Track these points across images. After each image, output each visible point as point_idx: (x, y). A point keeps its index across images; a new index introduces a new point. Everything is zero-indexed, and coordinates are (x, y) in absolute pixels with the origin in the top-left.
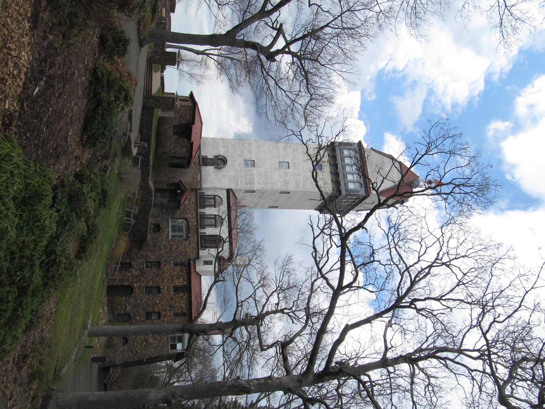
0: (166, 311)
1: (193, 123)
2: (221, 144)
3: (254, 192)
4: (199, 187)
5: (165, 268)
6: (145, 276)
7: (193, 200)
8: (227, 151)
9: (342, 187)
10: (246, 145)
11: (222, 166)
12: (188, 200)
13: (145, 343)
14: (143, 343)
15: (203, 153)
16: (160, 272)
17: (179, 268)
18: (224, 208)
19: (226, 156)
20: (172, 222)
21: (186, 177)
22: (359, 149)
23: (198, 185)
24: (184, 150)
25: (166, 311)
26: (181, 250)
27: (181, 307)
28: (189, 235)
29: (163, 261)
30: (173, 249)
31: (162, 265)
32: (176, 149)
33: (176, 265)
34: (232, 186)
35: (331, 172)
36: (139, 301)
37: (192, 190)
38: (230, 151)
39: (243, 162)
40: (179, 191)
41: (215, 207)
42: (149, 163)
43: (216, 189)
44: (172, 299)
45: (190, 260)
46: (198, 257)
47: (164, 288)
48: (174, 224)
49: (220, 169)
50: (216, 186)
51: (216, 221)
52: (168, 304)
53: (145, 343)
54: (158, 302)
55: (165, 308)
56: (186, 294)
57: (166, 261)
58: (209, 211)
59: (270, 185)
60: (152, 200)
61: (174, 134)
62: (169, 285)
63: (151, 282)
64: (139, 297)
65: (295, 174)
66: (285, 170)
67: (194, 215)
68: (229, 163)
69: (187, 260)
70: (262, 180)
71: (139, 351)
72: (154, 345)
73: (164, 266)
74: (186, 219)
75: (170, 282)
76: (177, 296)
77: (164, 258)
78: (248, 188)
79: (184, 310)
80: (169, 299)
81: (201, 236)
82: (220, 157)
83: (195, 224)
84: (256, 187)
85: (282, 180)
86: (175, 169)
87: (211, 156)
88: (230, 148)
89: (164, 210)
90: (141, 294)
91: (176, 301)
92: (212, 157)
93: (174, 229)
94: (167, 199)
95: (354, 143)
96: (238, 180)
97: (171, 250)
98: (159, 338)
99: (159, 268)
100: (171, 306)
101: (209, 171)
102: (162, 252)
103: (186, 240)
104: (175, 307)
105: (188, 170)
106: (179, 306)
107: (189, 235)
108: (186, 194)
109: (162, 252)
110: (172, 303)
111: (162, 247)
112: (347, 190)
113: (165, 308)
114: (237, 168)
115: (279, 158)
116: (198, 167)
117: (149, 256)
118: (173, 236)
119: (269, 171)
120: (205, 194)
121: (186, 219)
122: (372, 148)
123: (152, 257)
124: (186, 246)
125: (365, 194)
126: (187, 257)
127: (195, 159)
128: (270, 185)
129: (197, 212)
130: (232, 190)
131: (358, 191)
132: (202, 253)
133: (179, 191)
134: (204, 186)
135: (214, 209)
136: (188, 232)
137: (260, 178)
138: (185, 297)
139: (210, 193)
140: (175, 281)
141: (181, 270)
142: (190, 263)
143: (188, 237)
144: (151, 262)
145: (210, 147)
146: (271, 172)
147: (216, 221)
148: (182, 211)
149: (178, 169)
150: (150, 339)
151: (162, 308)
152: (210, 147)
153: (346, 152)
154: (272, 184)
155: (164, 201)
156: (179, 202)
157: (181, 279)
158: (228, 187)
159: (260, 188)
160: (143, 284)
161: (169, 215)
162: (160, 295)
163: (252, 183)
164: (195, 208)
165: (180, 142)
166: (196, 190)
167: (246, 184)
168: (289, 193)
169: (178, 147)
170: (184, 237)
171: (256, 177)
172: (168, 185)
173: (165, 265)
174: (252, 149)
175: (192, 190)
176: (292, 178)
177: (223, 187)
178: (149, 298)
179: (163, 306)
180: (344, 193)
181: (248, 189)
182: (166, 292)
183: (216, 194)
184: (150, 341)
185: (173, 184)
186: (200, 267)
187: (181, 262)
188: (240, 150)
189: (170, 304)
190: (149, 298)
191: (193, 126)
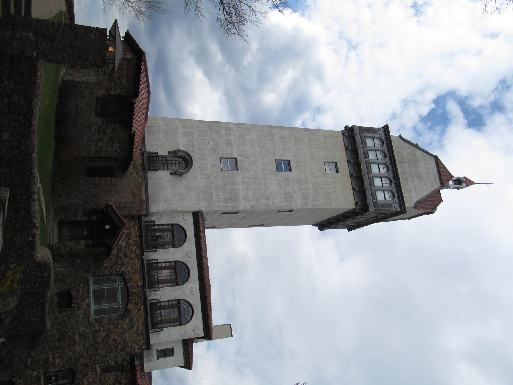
1: (136, 94)
2: (180, 130)
4: (144, 212)
7: (134, 237)
9: (370, 200)
10: (222, 132)
12: (126, 240)
15: (150, 148)
17: (113, 377)
18: (190, 245)
19: (189, 150)
20: (95, 283)
21: (117, 195)
22: (386, 138)
23: (142, 208)
24: (117, 146)
26: (114, 340)
28: (130, 306)
30: (99, 340)
31: (79, 376)
32: (100, 144)
33: (106, 370)
35: (351, 175)
37: (131, 218)
39: (218, 162)
40: (107, 227)
41: (174, 247)
43: (175, 212)
45: (132, 360)
48: (100, 287)
49: (181, 175)
50: (175, 206)
51: (179, 273)
57: (85, 365)
58: (164, 255)
59: (263, 201)
60: (49, 277)
61: (98, 114)
66: (284, 174)
67: (138, 266)
68: (196, 164)
69: (128, 358)
70: (251, 192)
77: (82, 361)
82: (180, 154)
83: (140, 283)
86: (97, 179)
87: (163, 152)
89: (79, 261)
92: (166, 154)
93: (99, 297)
94: (83, 242)
95: (379, 129)
101: (161, 180)
102: (78, 348)
103: (123, 317)
107: (130, 306)
109: (78, 348)
111: (77, 338)
112: (376, 204)
116: (141, 173)
117: (51, 360)
118: (97, 312)
120: (156, 223)
121: (122, 275)
122: (400, 136)
123: (57, 361)
124: (124, 331)
125: (399, 209)
126: (127, 353)
128: (263, 201)
129: (142, 260)
131: (389, 205)
132: (154, 339)
133: (107, 227)
134: (154, 208)
135: (172, 250)
136: (128, 302)
139: (165, 220)
142: (133, 367)
143: (126, 311)
146: (265, 178)
147: (179, 273)
148: (114, 260)
149: (103, 179)
153: (369, 143)
158: (195, 209)
159: (248, 208)
163: (235, 198)
164: (138, 252)
165: (108, 131)
166: (140, 217)
170: (121, 312)
172: (85, 213)
173: (85, 375)
174: (232, 138)
175: (131, 218)
177: (187, 209)
180: (371, 208)
181: (230, 209)
183: (174, 223)
186: (152, 364)
187: (116, 362)
188: (213, 139)
191: (136, 101)
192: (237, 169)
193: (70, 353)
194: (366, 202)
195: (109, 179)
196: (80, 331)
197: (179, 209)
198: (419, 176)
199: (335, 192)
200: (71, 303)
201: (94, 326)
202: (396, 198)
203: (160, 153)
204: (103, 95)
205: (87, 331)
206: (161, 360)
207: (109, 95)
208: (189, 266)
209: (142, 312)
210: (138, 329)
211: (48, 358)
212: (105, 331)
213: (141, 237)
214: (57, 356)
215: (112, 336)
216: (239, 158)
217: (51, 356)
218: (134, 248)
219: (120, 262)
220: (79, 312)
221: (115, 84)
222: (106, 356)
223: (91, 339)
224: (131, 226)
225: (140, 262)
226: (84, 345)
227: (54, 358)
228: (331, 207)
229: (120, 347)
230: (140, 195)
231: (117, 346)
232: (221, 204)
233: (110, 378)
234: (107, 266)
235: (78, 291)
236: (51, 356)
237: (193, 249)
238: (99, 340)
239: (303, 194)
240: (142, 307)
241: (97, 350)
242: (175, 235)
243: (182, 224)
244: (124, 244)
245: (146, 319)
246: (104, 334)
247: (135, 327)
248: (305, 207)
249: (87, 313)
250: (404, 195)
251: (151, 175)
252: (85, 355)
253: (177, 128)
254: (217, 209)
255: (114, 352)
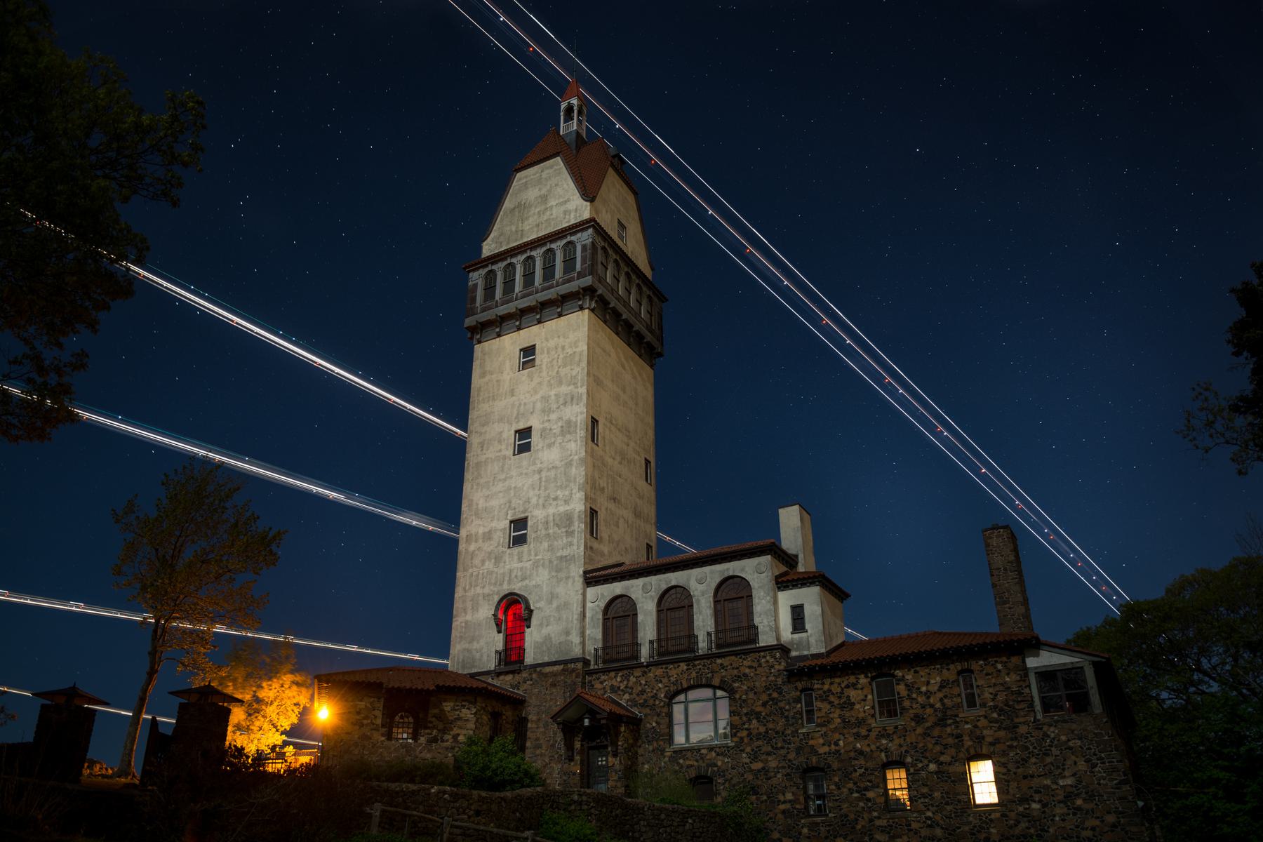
0: (959, 736)
2: (469, 617)
3: (593, 513)
4: (579, 665)
5: (826, 749)
6: (852, 816)
7: (617, 680)
8: (486, 597)
11: (523, 606)
13: (1079, 802)
14: (1079, 809)
16: (835, 765)
18: (634, 588)
19: (496, 599)
23: (573, 670)
25: (959, 736)
26: (764, 705)
27: (942, 687)
28: (716, 682)
29: (802, 759)
30: (762, 729)
32: (461, 738)
34: (577, 571)
35: (539, 322)
36: (938, 832)
38: (487, 591)
40: (586, 722)
42: (413, 792)
44: (918, 719)
46: (783, 649)
47: (886, 750)
50: (575, 617)
51: (675, 606)
52: (936, 732)
53: (1079, 802)
54: (932, 767)
55: (950, 740)
56: (899, 673)
57: (799, 750)
62: (873, 734)
63: (871, 794)
64: (924, 832)
65: (543, 411)
66: (535, 439)
67: (659, 671)
68: (517, 587)
71: (1111, 819)
72: (1082, 765)
73: (816, 753)
74: (671, 696)
75: (864, 732)
76: (907, 703)
77: (792, 756)
78: (579, 527)
79: (950, 672)
80: (919, 730)
81: (718, 646)
83: (683, 666)
84: (578, 505)
85: (559, 440)
86: (528, 744)
88: (479, 590)
90: (914, 825)
91: (923, 707)
96: (561, 557)
97: (765, 736)
98: (1055, 751)
99: (822, 770)
100: (941, 722)
102: (773, 764)
104: (945, 708)
105: (533, 701)
106: (940, 695)
107: (716, 682)
108: (592, 699)
109: (773, 764)
110: (932, 720)
113: (950, 740)
114: (528, 565)
115: (505, 457)
116: (525, 675)
117: (787, 806)
119: (537, 477)
120: (600, 645)
123: (789, 796)
127: (504, 683)
129: (649, 665)
130: (585, 573)
132: (766, 640)
133: (586, 722)
134: (577, 652)
135: (640, 618)
137: (556, 499)
138: (909, 677)
139: (595, 633)
140: (861, 715)
141: (823, 699)
144: (807, 798)
145: (475, 645)
146: (540, 471)
147: (675, 606)
148: (647, 711)
150: (1061, 783)
151: (953, 751)
152: (475, 645)
154: (569, 464)
155: (618, 767)
156: (616, 719)
157: (853, 693)
158: (579, 582)
159: (581, 495)
160: (878, 823)
161: (663, 751)
162: (909, 760)
163: (568, 518)
164: (638, 672)
166: (591, 673)
167: (570, 534)
168: (594, 422)
169: (456, 731)
171: (551, 510)
172: (571, 759)
173: (813, 751)
174: (481, 531)
176: (553, 417)
178: (924, 796)
179: (946, 746)
182: (897, 741)
184: (1069, 781)
185: (569, 747)
186: (812, 640)
188: (483, 562)
189: (935, 725)
190: (924, 796)
192: (526, 518)
193: (779, 776)
194: (578, 293)
195: (529, 725)
196: (748, 760)
197: (580, 609)
198: (544, 199)
199: (563, 348)
200: (705, 777)
201: (742, 738)
202: (573, 238)
203: (500, 646)
204: (383, 735)
205: (748, 749)
206: (807, 626)
207: (383, 726)
208: (664, 587)
209: (725, 661)
210: (750, 667)
211: (783, 812)
212: (750, 721)
213: (617, 670)
214: (781, 798)
215: (759, 709)
216: (510, 518)
217: (782, 807)
218: (633, 679)
219: (651, 702)
220: (719, 763)
221: (366, 718)
222: (787, 717)
223: (760, 743)
224: (600, 686)
225: (653, 668)
226: (769, 754)
227: (785, 802)
228: (586, 353)
229: (775, 695)
230: (554, 675)
231: (773, 699)
232: (575, 541)
233: (820, 710)
234: (657, 723)
235: (689, 766)
236: (782, 807)
237: (640, 582)
238: (762, 729)
239: (565, 404)
240: (719, 661)
241: (777, 733)
242: (619, 615)
243: (603, 604)
244: (627, 696)
245: (736, 654)
246: (754, 721)
247: (747, 671)
248: (585, 397)
249: (722, 751)
250: (573, 222)
251: (529, 659)
252: (783, 752)
253: (466, 622)
254: (582, 548)
255: (782, 704)
